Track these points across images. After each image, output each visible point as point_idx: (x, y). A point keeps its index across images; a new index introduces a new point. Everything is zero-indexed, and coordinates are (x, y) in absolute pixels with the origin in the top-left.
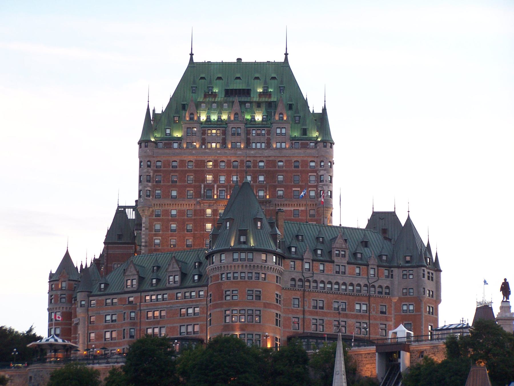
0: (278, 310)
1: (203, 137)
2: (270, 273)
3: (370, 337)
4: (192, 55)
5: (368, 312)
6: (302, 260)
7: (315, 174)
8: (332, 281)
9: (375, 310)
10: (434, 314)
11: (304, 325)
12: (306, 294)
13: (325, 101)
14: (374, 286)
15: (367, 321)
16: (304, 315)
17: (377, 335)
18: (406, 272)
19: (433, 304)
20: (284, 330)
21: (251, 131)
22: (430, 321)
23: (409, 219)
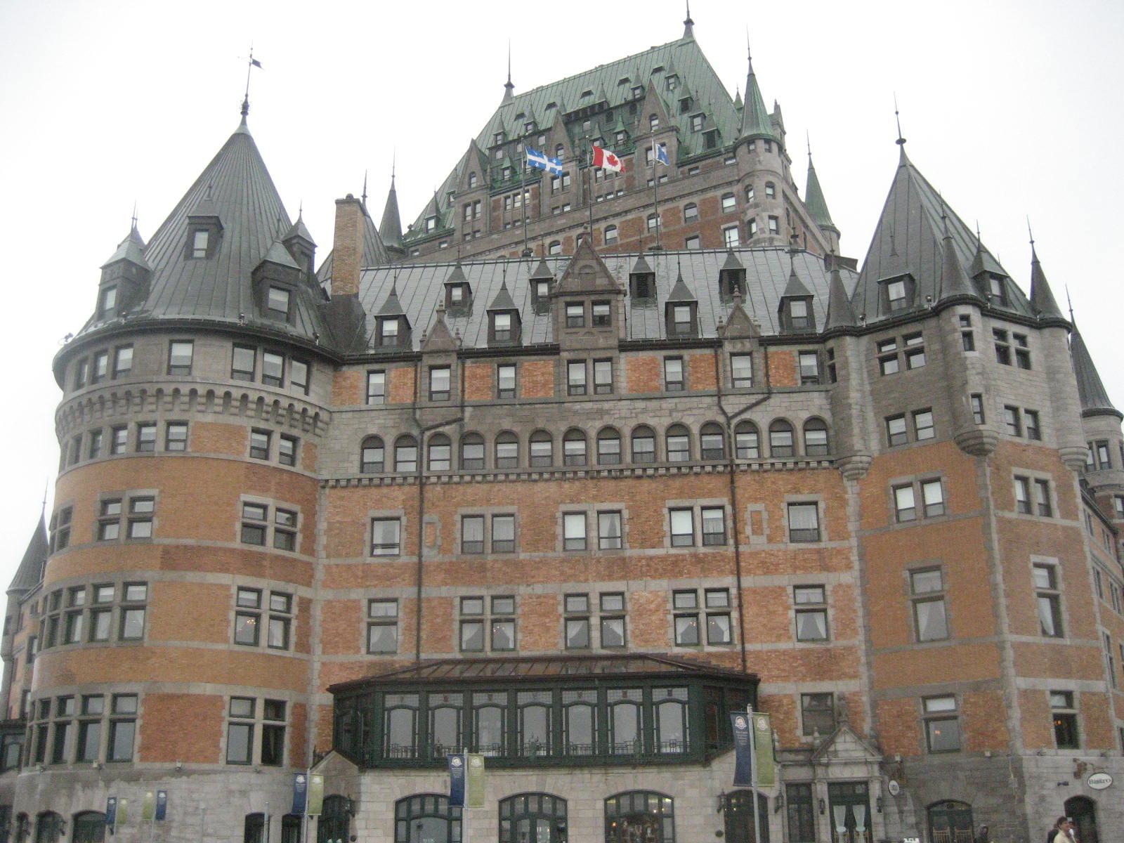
0: (262, 576)
1: (495, 214)
2: (209, 418)
3: (743, 648)
4: (509, 86)
5: (731, 541)
6: (414, 359)
7: (737, 223)
8: (550, 427)
9: (765, 525)
10: (1057, 513)
11: (419, 630)
12: (433, 493)
13: (750, 58)
14: (749, 427)
15: (729, 581)
16: (419, 584)
17: (779, 638)
18: (892, 347)
19: (1042, 469)
20: (325, 658)
21: (593, 173)
22: (1037, 547)
23: (905, 164)
